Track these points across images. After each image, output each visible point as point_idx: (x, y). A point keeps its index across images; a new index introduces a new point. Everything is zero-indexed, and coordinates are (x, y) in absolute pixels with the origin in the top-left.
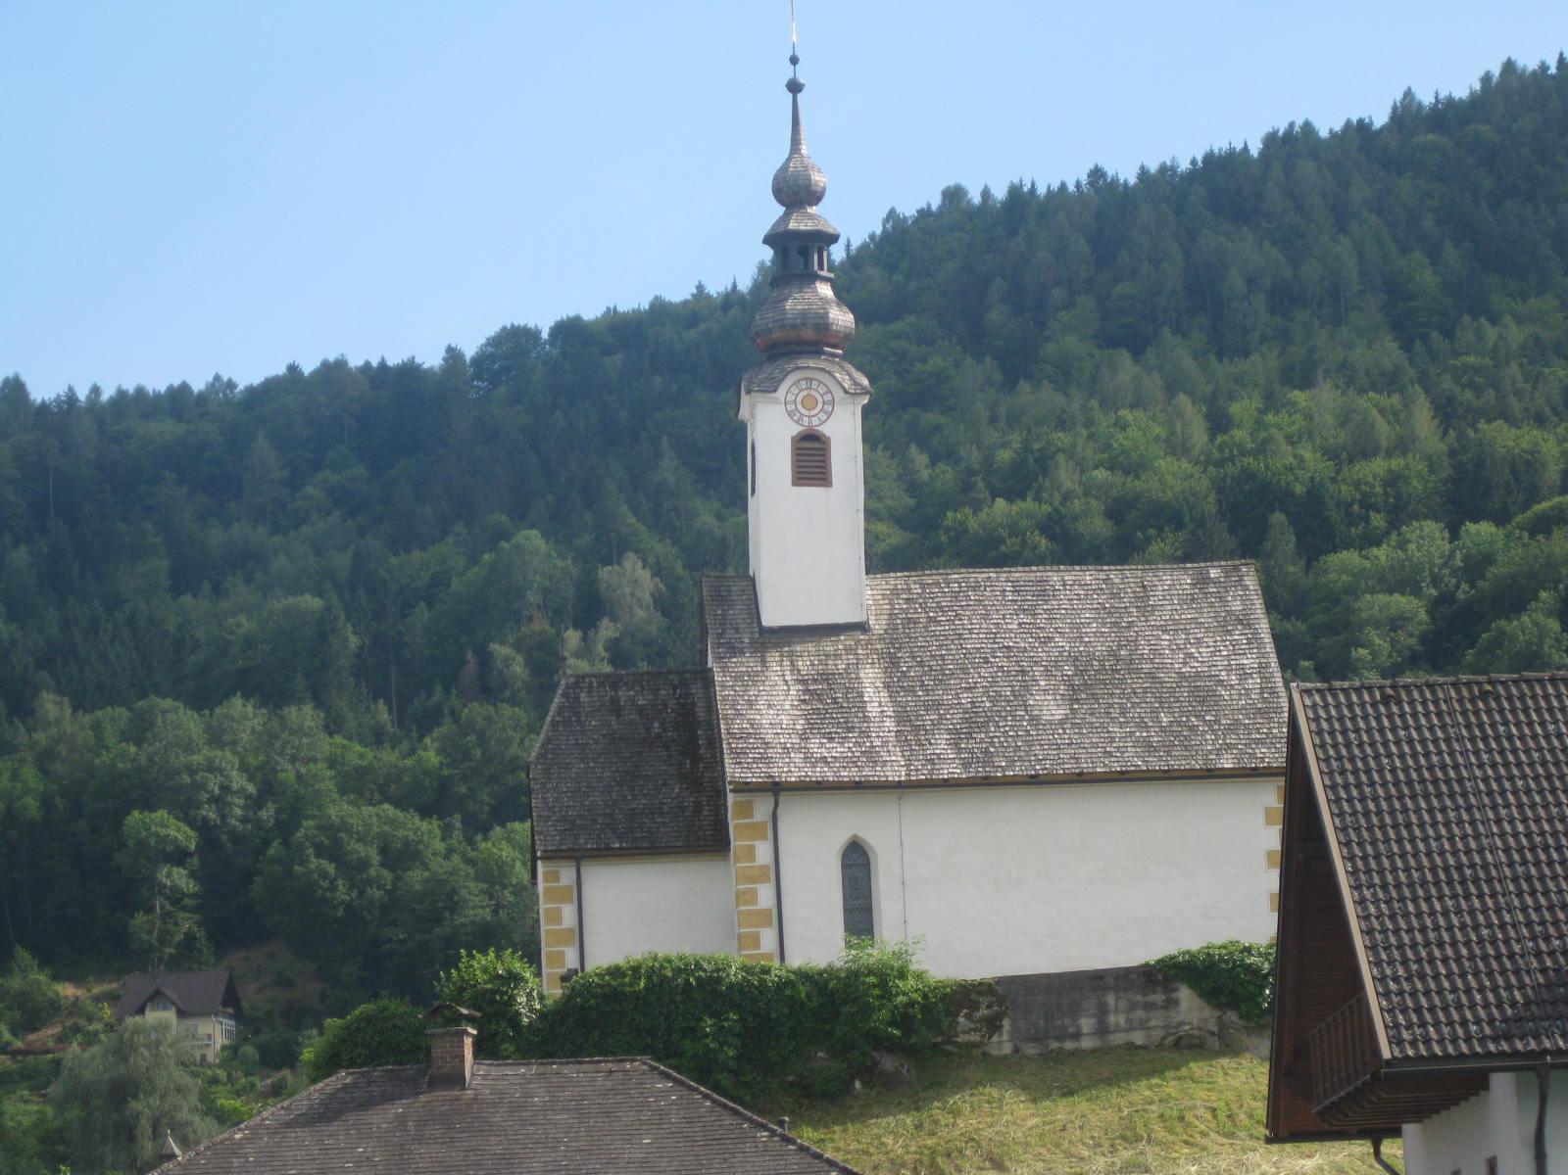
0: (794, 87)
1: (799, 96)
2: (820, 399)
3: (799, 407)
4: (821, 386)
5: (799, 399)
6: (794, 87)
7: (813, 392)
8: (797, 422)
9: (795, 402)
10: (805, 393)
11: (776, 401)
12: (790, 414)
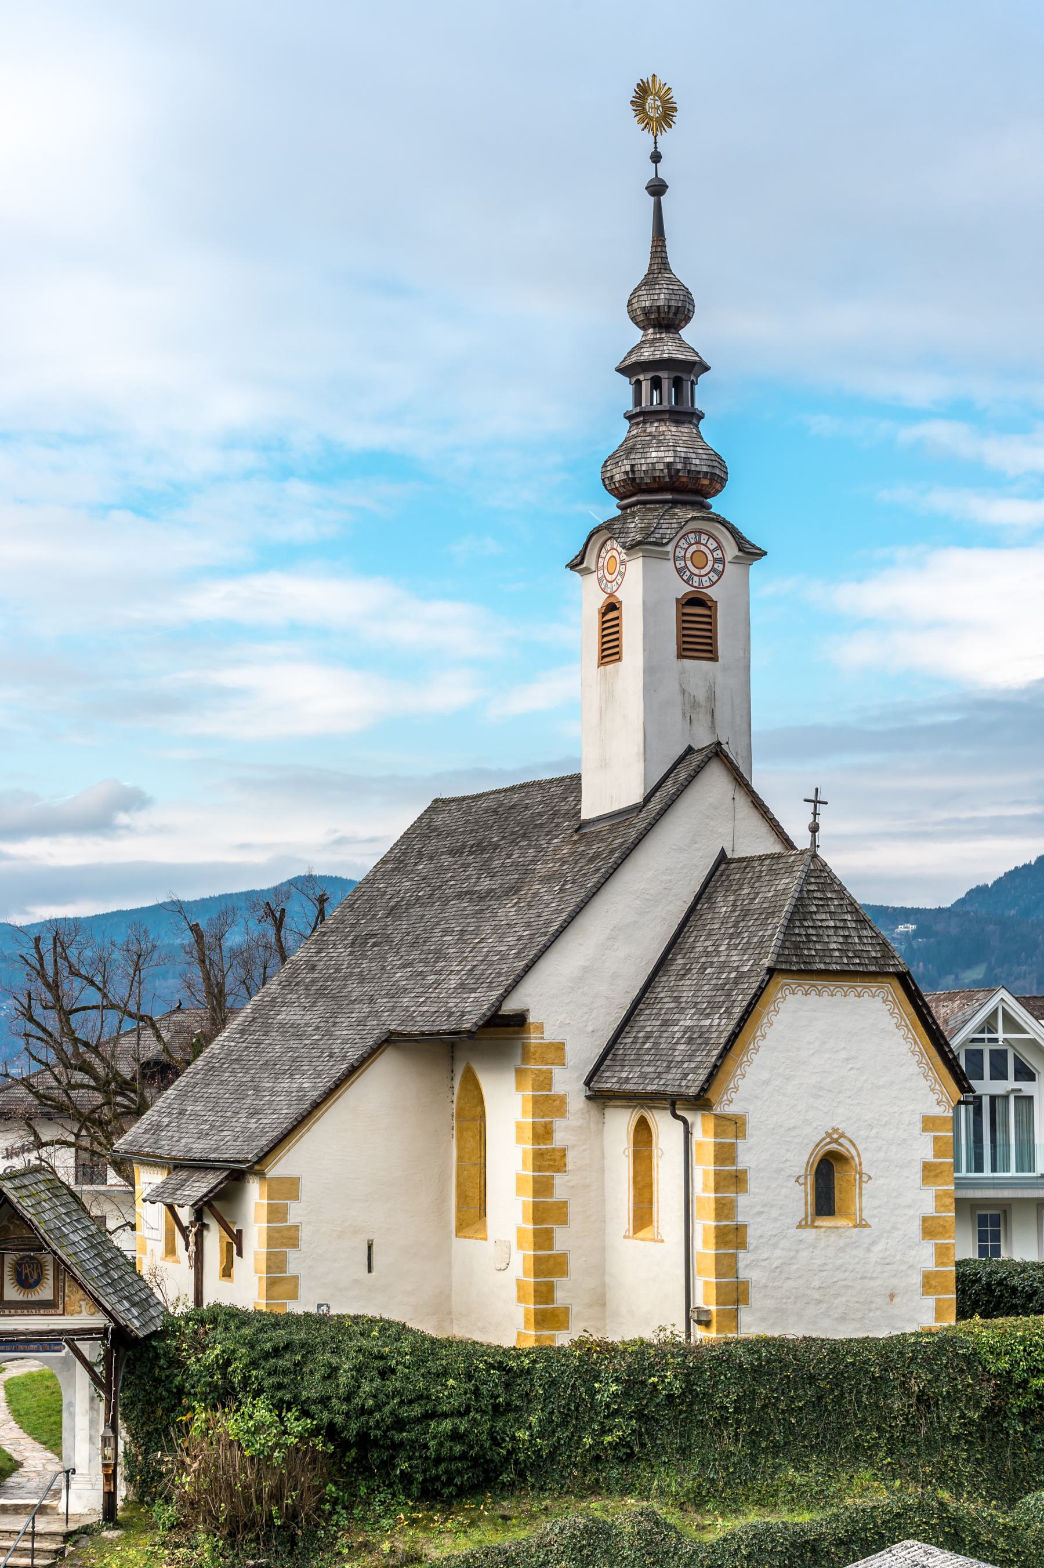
0: (657, 189)
1: (662, 198)
2: (710, 557)
3: (689, 563)
5: (688, 555)
6: (657, 189)
7: (703, 548)
9: (684, 558)
10: (694, 548)
11: (664, 556)
12: (679, 571)
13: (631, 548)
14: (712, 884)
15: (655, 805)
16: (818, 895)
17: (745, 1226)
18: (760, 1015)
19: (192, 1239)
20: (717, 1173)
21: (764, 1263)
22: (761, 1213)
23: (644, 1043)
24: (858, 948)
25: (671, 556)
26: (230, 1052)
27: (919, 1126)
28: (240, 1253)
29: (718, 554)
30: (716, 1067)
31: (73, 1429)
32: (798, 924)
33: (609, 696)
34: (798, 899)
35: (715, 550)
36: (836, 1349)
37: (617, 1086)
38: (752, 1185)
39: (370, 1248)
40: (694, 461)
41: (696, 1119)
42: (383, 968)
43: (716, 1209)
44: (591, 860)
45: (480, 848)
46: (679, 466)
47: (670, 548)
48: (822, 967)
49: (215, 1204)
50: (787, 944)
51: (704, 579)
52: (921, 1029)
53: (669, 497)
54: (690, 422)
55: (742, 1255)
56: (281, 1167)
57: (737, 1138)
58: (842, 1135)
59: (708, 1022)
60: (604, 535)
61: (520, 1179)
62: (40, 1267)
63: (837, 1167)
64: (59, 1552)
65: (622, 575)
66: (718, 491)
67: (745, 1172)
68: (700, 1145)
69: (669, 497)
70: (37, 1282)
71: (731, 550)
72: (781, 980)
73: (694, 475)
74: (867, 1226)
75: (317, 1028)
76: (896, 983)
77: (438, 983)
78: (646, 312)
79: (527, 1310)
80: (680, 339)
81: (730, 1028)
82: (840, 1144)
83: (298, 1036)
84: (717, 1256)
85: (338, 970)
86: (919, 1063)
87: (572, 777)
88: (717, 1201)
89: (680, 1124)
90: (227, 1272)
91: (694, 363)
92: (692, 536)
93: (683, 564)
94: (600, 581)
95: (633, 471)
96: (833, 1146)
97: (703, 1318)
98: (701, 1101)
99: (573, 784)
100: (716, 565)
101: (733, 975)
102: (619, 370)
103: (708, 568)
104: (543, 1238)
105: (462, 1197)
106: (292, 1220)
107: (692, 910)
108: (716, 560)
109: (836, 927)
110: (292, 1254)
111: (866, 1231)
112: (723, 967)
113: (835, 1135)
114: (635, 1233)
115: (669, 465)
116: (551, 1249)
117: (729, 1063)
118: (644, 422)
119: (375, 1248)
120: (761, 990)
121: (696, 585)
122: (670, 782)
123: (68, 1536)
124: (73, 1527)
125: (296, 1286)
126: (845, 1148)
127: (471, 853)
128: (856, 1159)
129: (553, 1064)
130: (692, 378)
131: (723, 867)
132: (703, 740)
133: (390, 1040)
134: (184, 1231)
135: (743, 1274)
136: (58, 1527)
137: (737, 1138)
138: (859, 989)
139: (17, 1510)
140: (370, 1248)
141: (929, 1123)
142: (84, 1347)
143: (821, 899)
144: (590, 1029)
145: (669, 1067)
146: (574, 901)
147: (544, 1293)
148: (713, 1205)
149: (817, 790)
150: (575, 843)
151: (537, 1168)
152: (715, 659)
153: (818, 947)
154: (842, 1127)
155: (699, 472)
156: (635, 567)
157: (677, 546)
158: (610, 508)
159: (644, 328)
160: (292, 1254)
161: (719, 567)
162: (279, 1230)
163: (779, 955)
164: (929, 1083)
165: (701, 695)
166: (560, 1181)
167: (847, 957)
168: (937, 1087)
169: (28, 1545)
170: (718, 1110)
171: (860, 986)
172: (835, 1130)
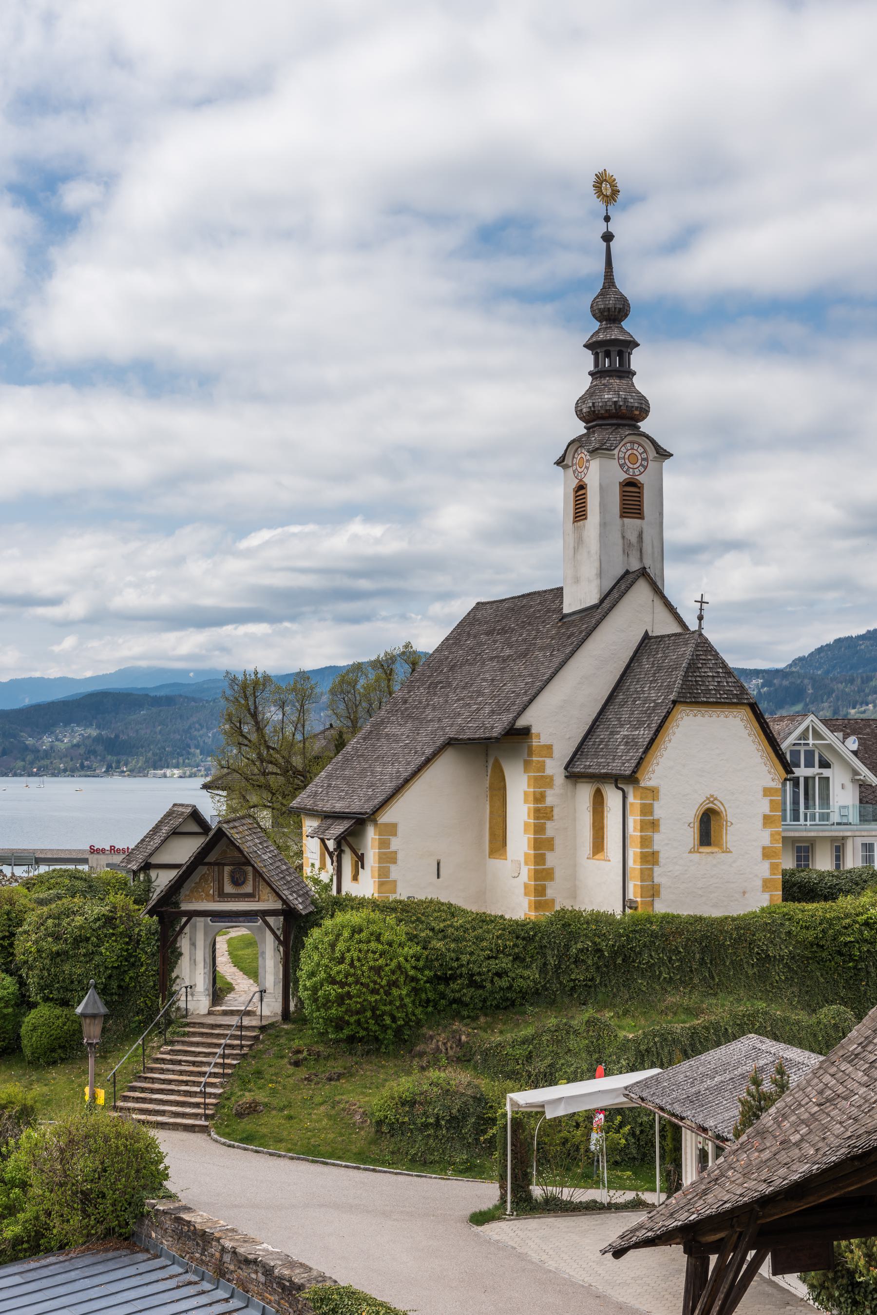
0: (608, 237)
2: (639, 458)
4: (640, 447)
5: (626, 456)
6: (608, 237)
7: (635, 452)
8: (625, 472)
10: (630, 452)
11: (612, 457)
12: (621, 466)
13: (593, 452)
14: (640, 651)
15: (606, 604)
16: (703, 657)
17: (658, 852)
18: (668, 728)
19: (335, 858)
20: (641, 821)
21: (669, 874)
22: (667, 844)
23: (599, 745)
24: (727, 688)
25: (616, 457)
26: (357, 750)
27: (762, 793)
28: (363, 867)
29: (644, 455)
30: (641, 758)
31: (265, 967)
32: (690, 674)
33: (579, 541)
34: (690, 660)
35: (642, 453)
36: (711, 923)
37: (583, 770)
38: (663, 828)
39: (438, 864)
40: (630, 400)
41: (630, 790)
42: (447, 701)
43: (641, 842)
44: (569, 637)
45: (503, 631)
46: (621, 403)
47: (616, 452)
48: (705, 699)
49: (348, 838)
50: (684, 686)
51: (636, 470)
52: (763, 737)
53: (614, 421)
54: (628, 377)
55: (656, 869)
56: (385, 818)
57: (654, 800)
58: (716, 799)
59: (637, 732)
60: (577, 445)
61: (526, 824)
62: (245, 874)
63: (712, 817)
64: (256, 1038)
65: (587, 468)
66: (644, 418)
67: (658, 820)
68: (632, 804)
69: (614, 421)
70: (243, 883)
71: (652, 453)
72: (680, 708)
73: (631, 408)
74: (730, 852)
75: (408, 736)
76: (748, 709)
77: (478, 710)
78: (601, 311)
79: (530, 901)
80: (622, 327)
81: (650, 736)
82: (715, 804)
83: (397, 742)
84: (641, 869)
85: (420, 703)
86: (762, 756)
87: (557, 589)
88: (641, 837)
89: (620, 793)
90: (355, 878)
91: (630, 342)
92: (629, 445)
93: (623, 462)
94: (574, 472)
95: (594, 406)
96: (711, 805)
97: (634, 905)
98: (632, 779)
99: (558, 593)
100: (643, 462)
101: (652, 705)
102: (585, 346)
103: (638, 464)
104: (539, 859)
105: (492, 834)
106: (393, 848)
107: (628, 667)
108: (643, 459)
109: (713, 677)
110: (393, 868)
111: (729, 855)
112: (646, 701)
113: (712, 799)
114: (593, 856)
115: (615, 402)
116: (545, 865)
117: (649, 755)
118: (601, 377)
119: (441, 865)
120: (669, 713)
121: (631, 474)
122: (615, 591)
123: (263, 1028)
124: (264, 1023)
125: (395, 886)
126: (717, 806)
127: (499, 633)
128: (724, 813)
129: (546, 757)
130: (629, 350)
131: (646, 641)
132: (635, 566)
133: (451, 743)
134: (331, 854)
135: (656, 880)
136: (255, 1022)
137: (654, 800)
138: (727, 713)
139: (232, 1013)
140: (438, 864)
141: (767, 792)
142: (271, 920)
143: (704, 660)
144: (568, 736)
145: (614, 759)
146: (557, 661)
147: (540, 891)
148: (639, 840)
149: (702, 595)
150: (559, 627)
151: (536, 818)
152: (642, 518)
153: (702, 688)
154: (716, 794)
155: (633, 407)
156: (595, 465)
157: (620, 451)
158: (579, 428)
159: (600, 321)
160: (393, 868)
161: (645, 463)
162: (385, 854)
163: (679, 693)
164: (767, 768)
165: (633, 539)
166: (549, 825)
167: (720, 694)
168: (772, 771)
169: (239, 1033)
170: (642, 784)
171: (727, 711)
172: (712, 796)
